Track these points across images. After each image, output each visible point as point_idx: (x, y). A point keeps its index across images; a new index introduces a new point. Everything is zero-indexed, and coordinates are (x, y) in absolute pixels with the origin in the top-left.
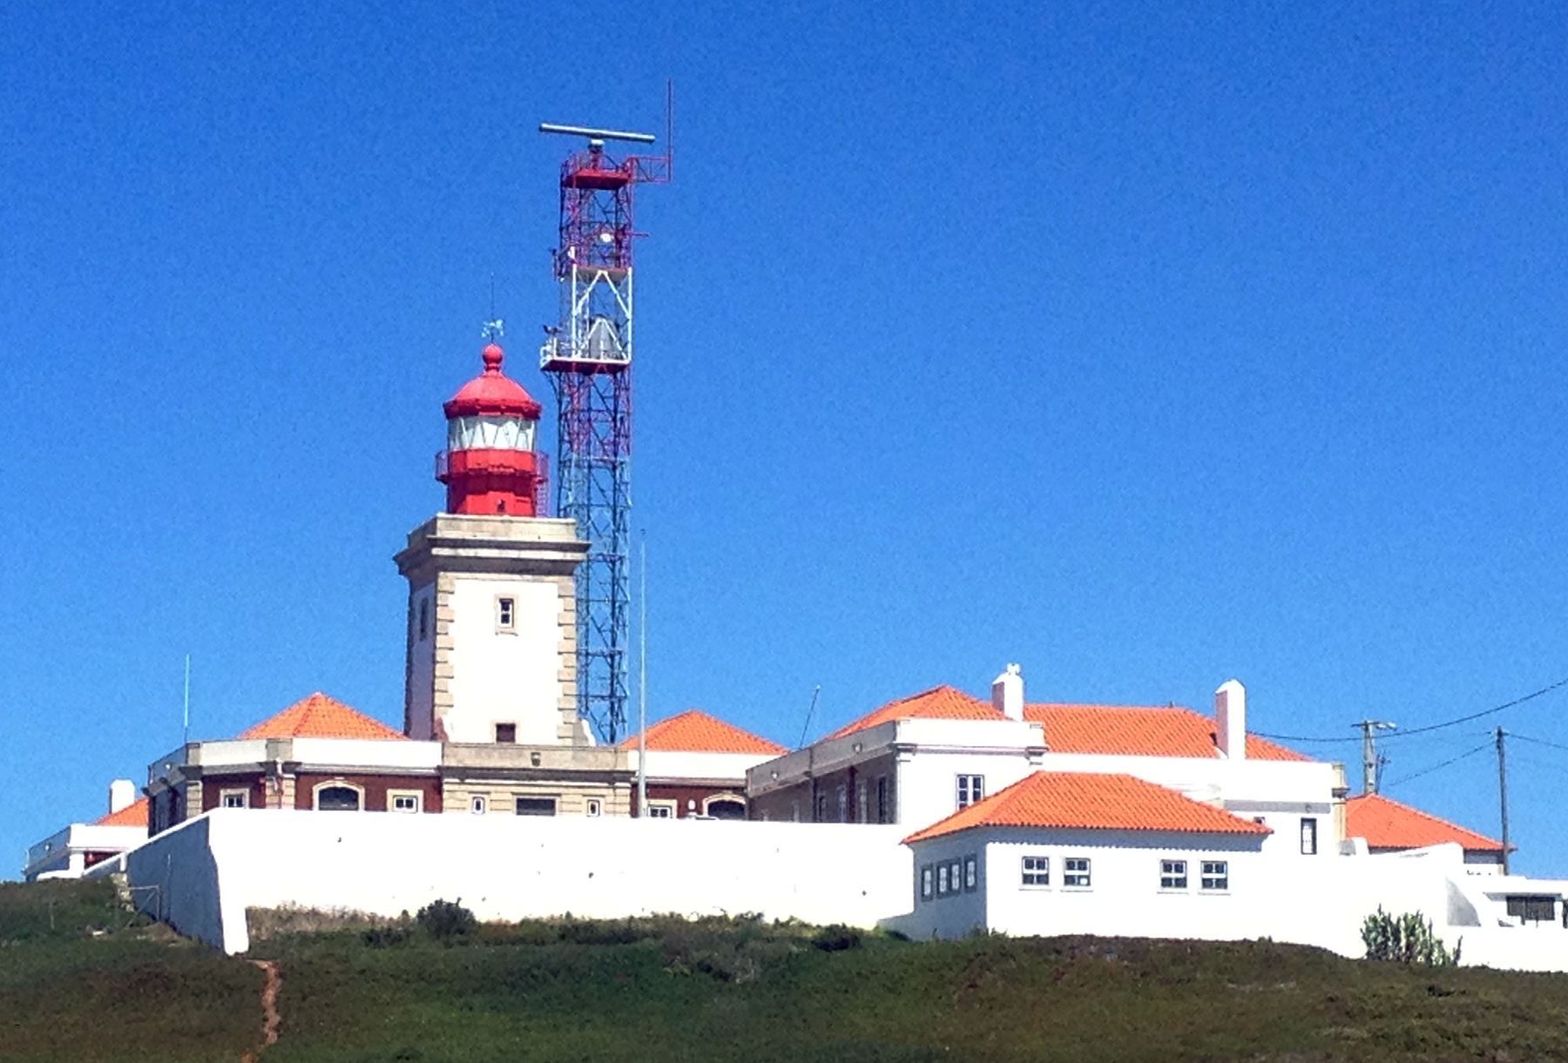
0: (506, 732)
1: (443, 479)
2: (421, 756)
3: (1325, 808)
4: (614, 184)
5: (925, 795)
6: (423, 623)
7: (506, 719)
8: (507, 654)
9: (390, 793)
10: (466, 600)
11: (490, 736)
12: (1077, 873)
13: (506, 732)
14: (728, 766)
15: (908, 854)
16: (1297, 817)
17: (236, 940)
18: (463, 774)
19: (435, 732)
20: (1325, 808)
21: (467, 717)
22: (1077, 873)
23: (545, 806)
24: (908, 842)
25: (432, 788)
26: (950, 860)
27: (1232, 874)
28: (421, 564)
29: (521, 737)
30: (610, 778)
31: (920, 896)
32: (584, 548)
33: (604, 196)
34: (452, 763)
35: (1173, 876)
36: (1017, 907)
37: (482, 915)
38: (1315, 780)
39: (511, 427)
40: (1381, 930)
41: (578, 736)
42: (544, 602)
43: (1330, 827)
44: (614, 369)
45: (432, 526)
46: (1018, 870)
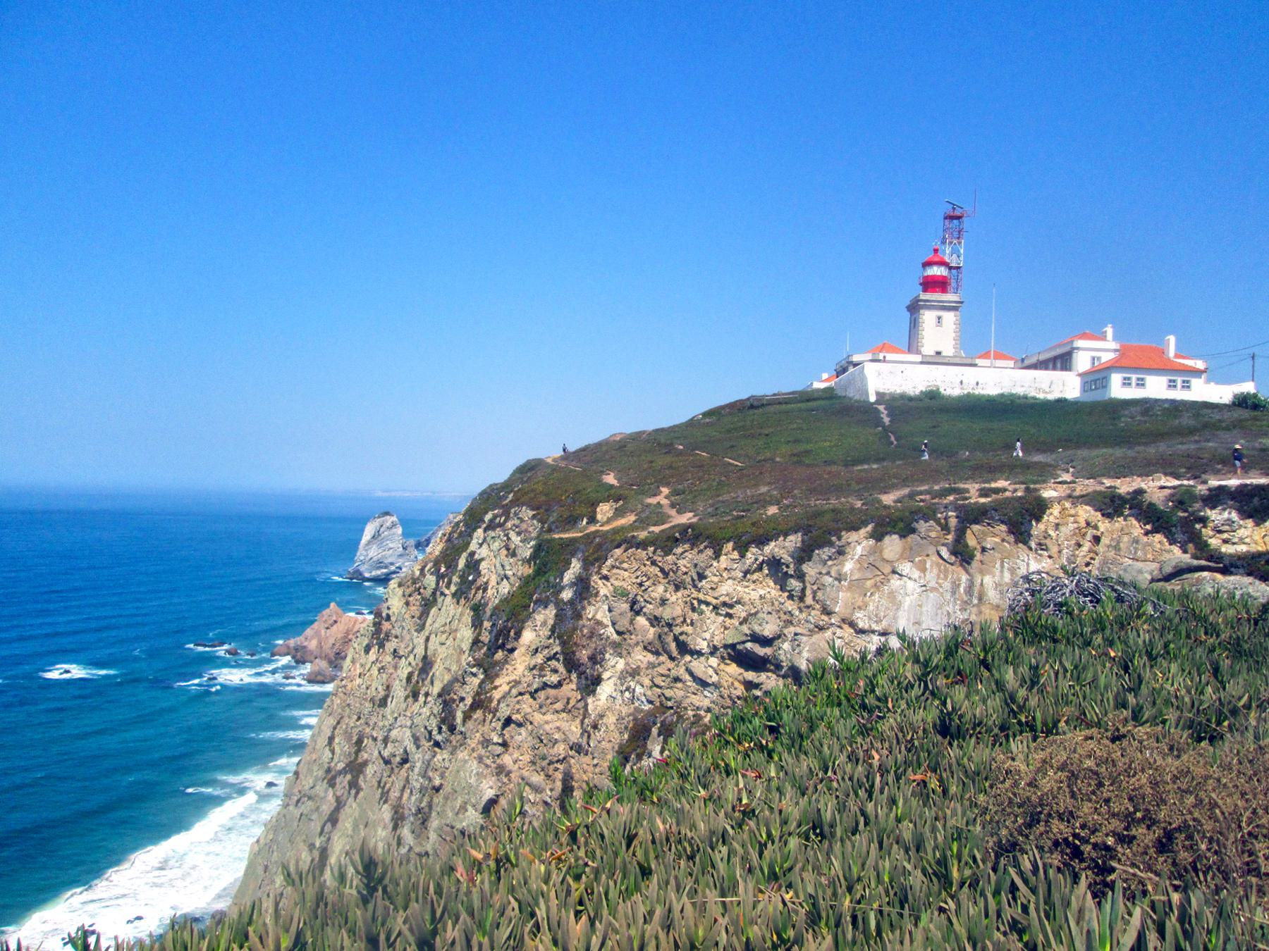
4: (959, 218)
5: (1082, 362)
6: (914, 325)
10: (928, 317)
11: (932, 353)
15: (1078, 380)
17: (872, 399)
21: (928, 349)
22: (1141, 384)
24: (1079, 375)
28: (914, 308)
31: (1084, 390)
33: (955, 222)
35: (1172, 385)
39: (943, 268)
44: (958, 268)
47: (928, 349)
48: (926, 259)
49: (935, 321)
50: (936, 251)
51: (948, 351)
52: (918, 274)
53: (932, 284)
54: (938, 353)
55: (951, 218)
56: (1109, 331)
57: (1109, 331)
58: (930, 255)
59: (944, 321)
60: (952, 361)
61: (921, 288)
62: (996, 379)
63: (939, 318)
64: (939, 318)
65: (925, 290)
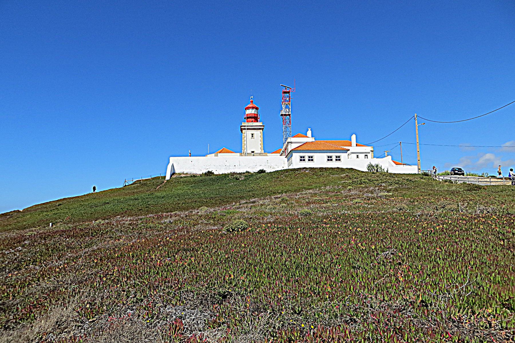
3: (369, 153)
4: (288, 92)
12: (311, 159)
16: (364, 155)
20: (369, 153)
22: (311, 159)
27: (341, 158)
28: (241, 130)
33: (288, 94)
35: (330, 159)
37: (216, 173)
38: (368, 149)
40: (370, 166)
42: (258, 134)
43: (369, 155)
44: (289, 115)
46: (299, 159)
49: (251, 136)
51: (258, 150)
54: (253, 152)
55: (285, 92)
56: (309, 133)
57: (309, 133)
59: (255, 136)
62: (275, 163)
63: (252, 134)
64: (252, 134)
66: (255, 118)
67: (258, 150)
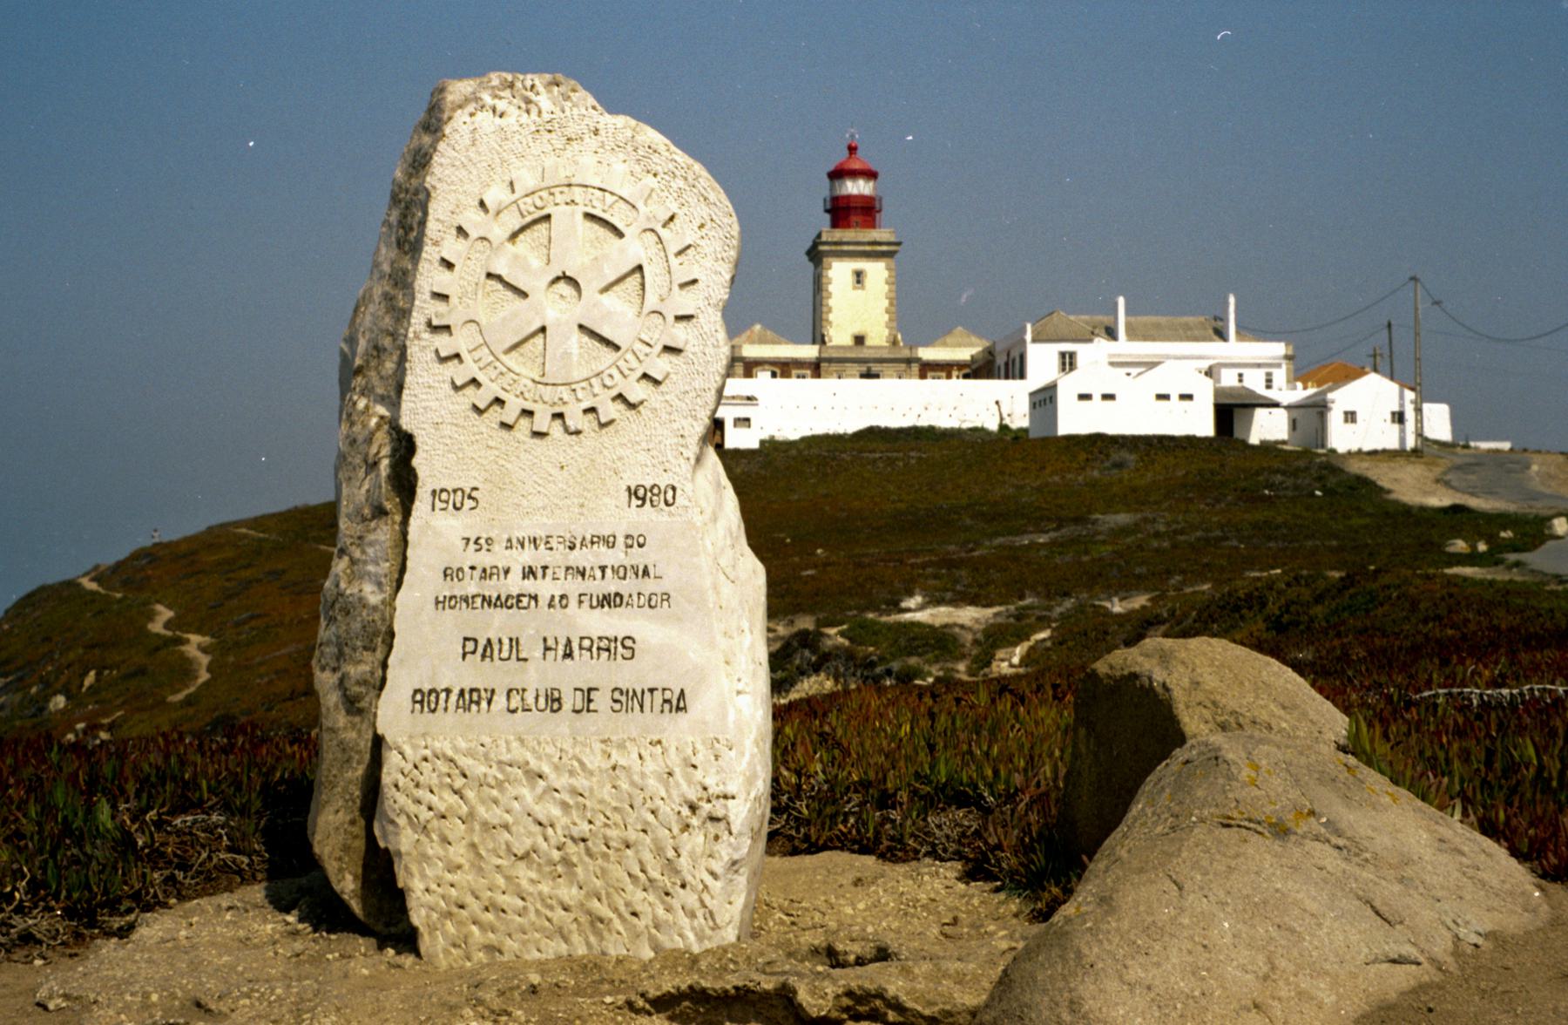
0: (859, 340)
1: (827, 211)
2: (809, 352)
6: (818, 287)
7: (857, 330)
8: (859, 299)
9: (794, 372)
10: (839, 272)
11: (849, 341)
13: (859, 340)
14: (964, 354)
18: (830, 360)
19: (819, 338)
20: (1279, 366)
21: (839, 335)
23: (877, 376)
25: (816, 368)
26: (1044, 399)
28: (816, 255)
29: (868, 342)
30: (909, 361)
32: (898, 244)
34: (824, 355)
36: (1073, 421)
41: (895, 343)
42: (877, 271)
45: (819, 236)
47: (839, 335)
48: (831, 168)
49: (850, 279)
50: (852, 149)
51: (879, 336)
52: (823, 189)
53: (842, 212)
58: (839, 157)
60: (885, 354)
61: (828, 217)
63: (859, 276)
65: (835, 224)
66: (866, 211)
67: (879, 336)
